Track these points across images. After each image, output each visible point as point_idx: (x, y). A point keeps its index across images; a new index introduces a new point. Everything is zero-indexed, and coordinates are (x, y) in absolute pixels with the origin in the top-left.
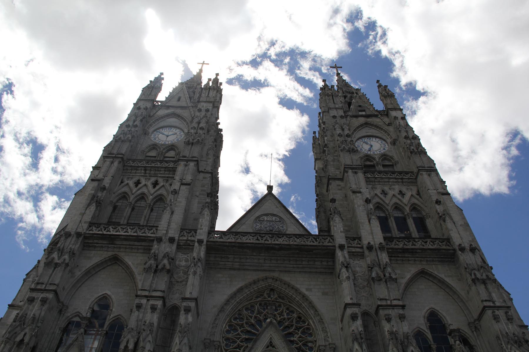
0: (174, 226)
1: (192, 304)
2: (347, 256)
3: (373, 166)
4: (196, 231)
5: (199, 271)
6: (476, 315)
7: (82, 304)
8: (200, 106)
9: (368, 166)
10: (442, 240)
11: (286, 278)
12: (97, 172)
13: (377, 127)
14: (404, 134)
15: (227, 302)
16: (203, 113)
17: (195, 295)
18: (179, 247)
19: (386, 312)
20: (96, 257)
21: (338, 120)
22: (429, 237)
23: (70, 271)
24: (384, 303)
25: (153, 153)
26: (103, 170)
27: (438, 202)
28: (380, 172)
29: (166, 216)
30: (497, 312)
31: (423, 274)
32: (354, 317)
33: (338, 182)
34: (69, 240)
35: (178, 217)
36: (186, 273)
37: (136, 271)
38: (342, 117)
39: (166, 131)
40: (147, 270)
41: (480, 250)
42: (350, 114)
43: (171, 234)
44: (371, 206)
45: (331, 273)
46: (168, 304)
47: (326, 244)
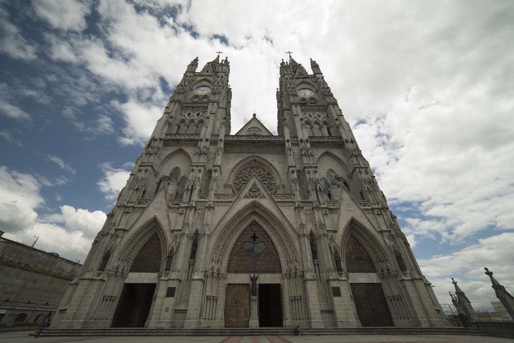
0: (208, 133)
1: (218, 168)
2: (290, 145)
3: (306, 103)
4: (219, 135)
5: (221, 153)
6: (351, 172)
7: (166, 171)
8: (218, 74)
9: (303, 103)
10: (337, 138)
11: (262, 156)
12: (167, 110)
13: (309, 83)
14: (322, 86)
15: (235, 167)
16: (220, 78)
17: (219, 164)
18: (211, 143)
19: (308, 169)
20: (171, 150)
21: (289, 80)
22: (331, 136)
23: (158, 157)
24: (307, 166)
25: (196, 100)
26: (170, 108)
27: (337, 120)
28: (309, 106)
29: (204, 129)
30: (361, 170)
31: (327, 153)
32: (293, 172)
33: (288, 111)
34: (156, 142)
35: (210, 129)
36: (215, 155)
37: (191, 155)
38: (291, 79)
39: (202, 89)
40: (195, 154)
41: (356, 143)
42: (295, 77)
43: (207, 137)
44: (303, 122)
45: (283, 153)
46: (207, 169)
47: (281, 140)
